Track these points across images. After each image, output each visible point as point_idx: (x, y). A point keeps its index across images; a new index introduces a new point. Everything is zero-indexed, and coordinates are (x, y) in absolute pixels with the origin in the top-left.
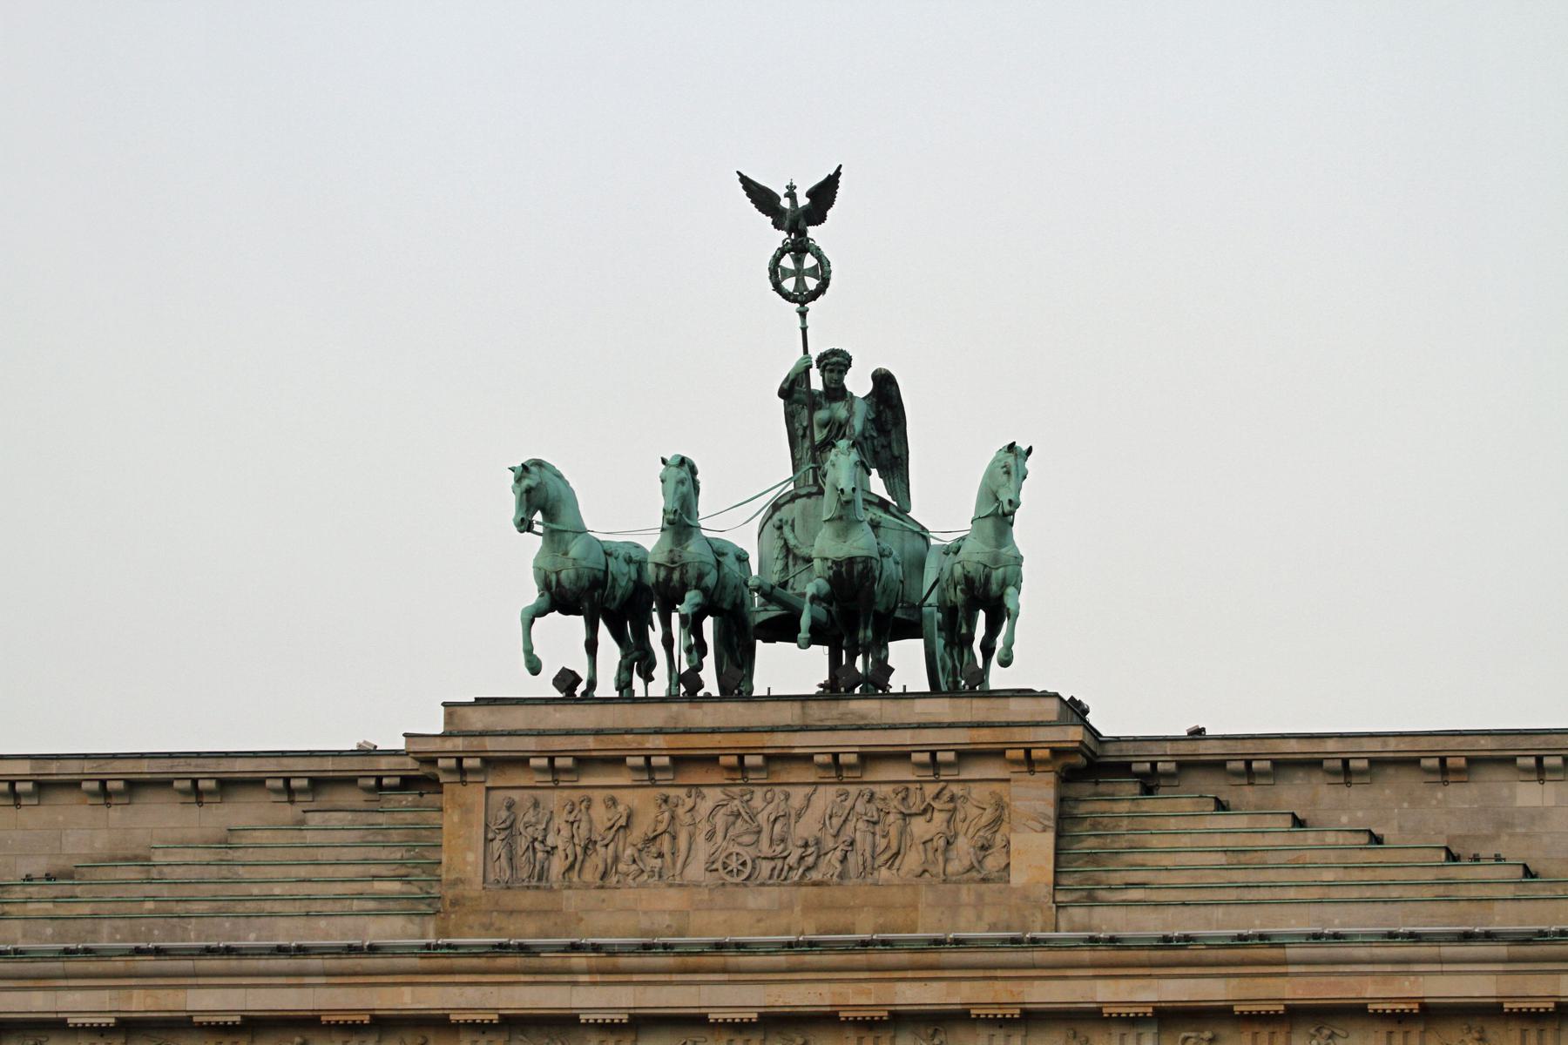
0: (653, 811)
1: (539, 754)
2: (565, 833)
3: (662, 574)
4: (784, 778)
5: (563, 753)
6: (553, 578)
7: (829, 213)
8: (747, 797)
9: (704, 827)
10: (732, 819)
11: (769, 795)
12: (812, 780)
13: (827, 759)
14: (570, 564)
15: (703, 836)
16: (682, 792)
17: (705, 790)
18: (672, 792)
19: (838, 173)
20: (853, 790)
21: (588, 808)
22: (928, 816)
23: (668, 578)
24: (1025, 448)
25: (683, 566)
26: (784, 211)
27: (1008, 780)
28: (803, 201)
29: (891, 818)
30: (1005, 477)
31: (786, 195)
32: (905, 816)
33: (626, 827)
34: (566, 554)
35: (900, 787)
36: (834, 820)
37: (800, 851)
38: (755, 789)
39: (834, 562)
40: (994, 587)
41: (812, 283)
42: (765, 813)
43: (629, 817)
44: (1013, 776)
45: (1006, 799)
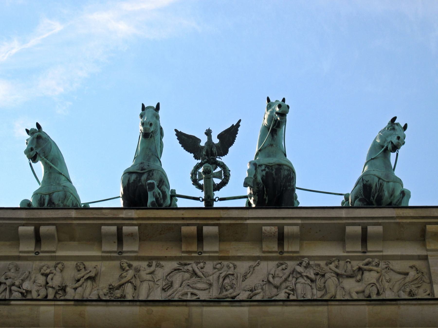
0: (117, 273)
1: (27, 222)
2: (41, 280)
3: (134, 177)
4: (232, 253)
5: (47, 222)
6: (47, 198)
7: (230, 149)
8: (202, 264)
9: (162, 283)
10: (187, 275)
11: (218, 266)
12: (257, 253)
13: (274, 229)
14: (61, 188)
15: (159, 289)
16: (144, 264)
17: (162, 263)
18: (135, 264)
19: (238, 125)
20: (291, 264)
21: (61, 271)
22: (359, 277)
23: (138, 180)
24: (403, 126)
25: (151, 171)
26: (203, 147)
27: (425, 258)
28: (216, 141)
29: (327, 275)
30: (392, 131)
31: (206, 133)
32: (338, 275)
33: (92, 279)
34: (59, 184)
35: (334, 259)
36: (277, 279)
37: (250, 293)
38: (207, 262)
39: (267, 166)
40: (386, 194)
41: (217, 181)
42: (215, 276)
43: (96, 275)
44: (429, 253)
45: (425, 270)
